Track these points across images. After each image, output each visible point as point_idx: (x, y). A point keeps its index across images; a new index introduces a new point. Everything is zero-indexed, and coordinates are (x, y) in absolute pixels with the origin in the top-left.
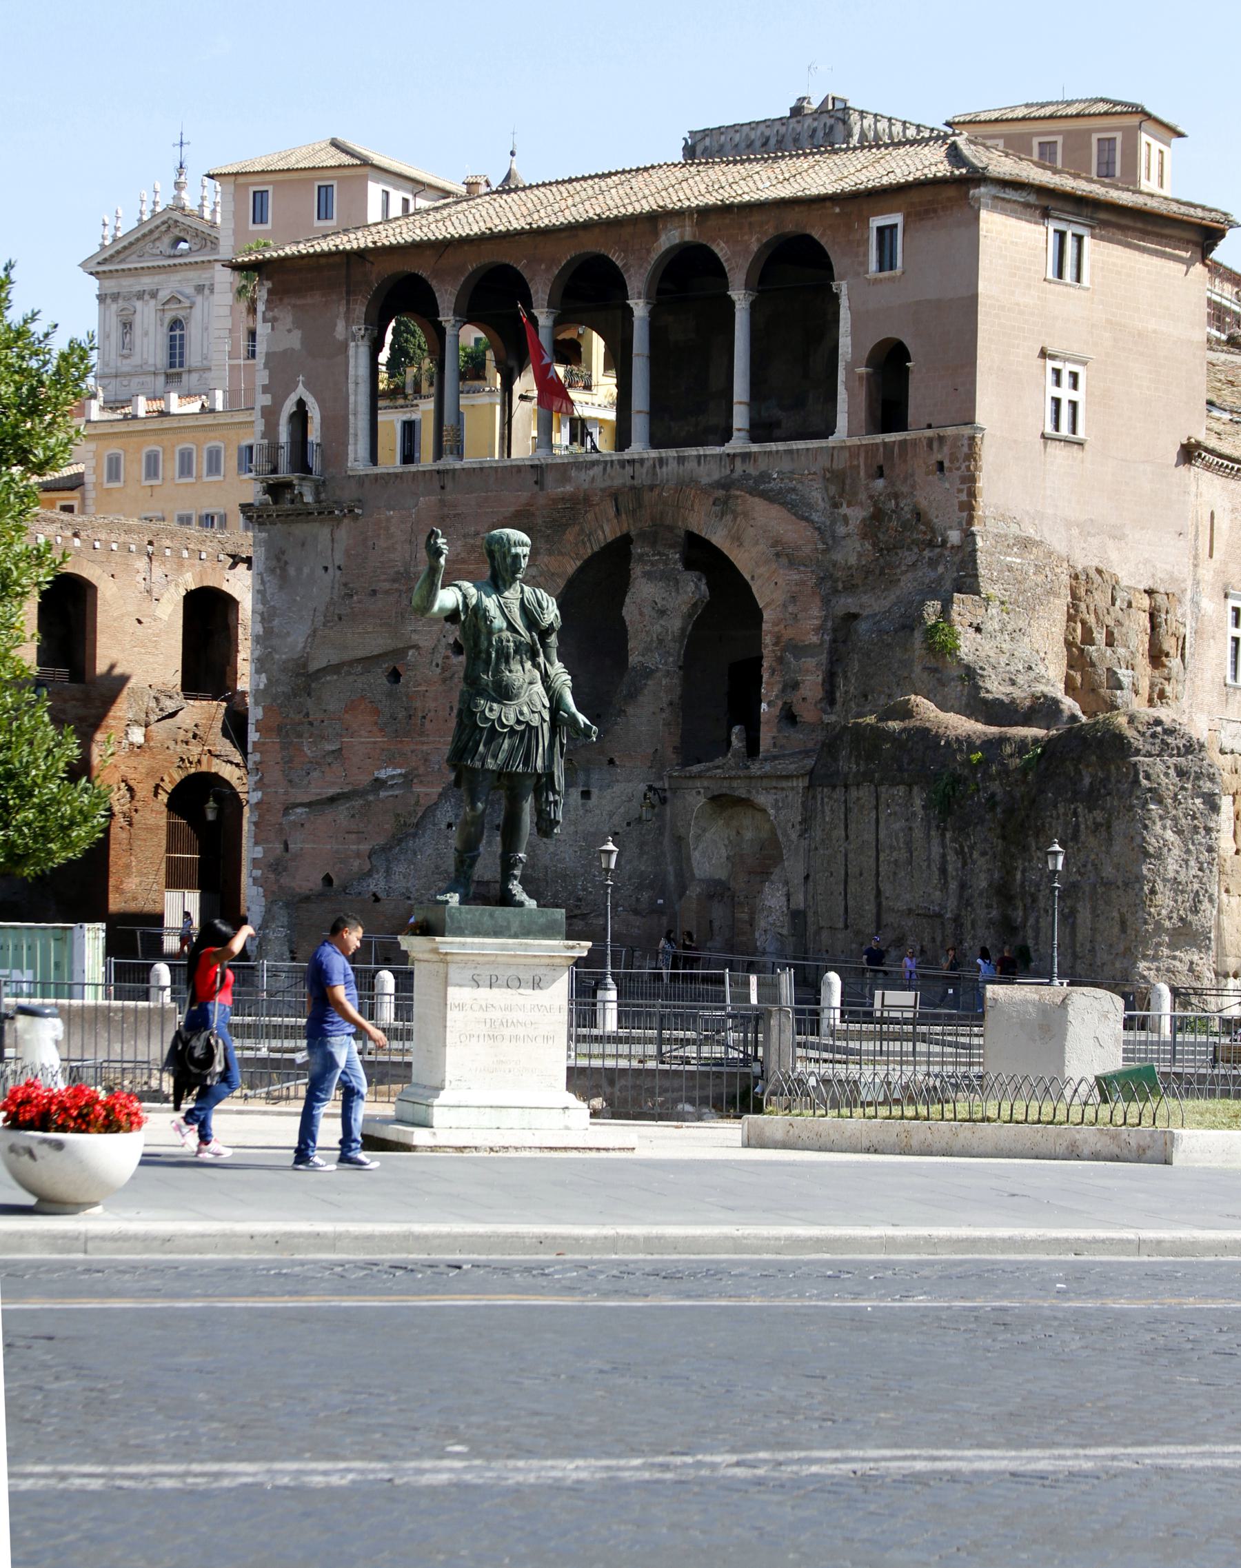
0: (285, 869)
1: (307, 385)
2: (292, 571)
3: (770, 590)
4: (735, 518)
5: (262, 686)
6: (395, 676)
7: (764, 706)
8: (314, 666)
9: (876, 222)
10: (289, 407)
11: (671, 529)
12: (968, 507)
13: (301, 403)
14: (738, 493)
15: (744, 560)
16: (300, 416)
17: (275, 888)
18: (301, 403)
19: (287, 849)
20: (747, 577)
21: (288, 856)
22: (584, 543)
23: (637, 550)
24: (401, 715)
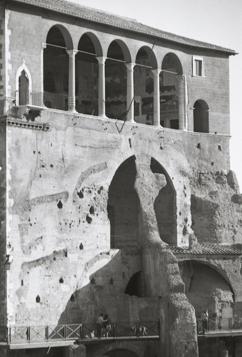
0: (22, 294)
1: (27, 65)
2: (22, 151)
3: (179, 184)
4: (167, 156)
5: (12, 205)
6: (60, 205)
7: (178, 226)
8: (32, 197)
9: (196, 57)
10: (19, 74)
11: (147, 156)
12: (228, 162)
13: (24, 72)
14: (168, 146)
15: (171, 171)
16: (23, 80)
17: (19, 304)
18: (24, 72)
19: (22, 284)
20: (171, 178)
21: (23, 287)
22: (121, 156)
23: (137, 162)
24: (63, 223)
